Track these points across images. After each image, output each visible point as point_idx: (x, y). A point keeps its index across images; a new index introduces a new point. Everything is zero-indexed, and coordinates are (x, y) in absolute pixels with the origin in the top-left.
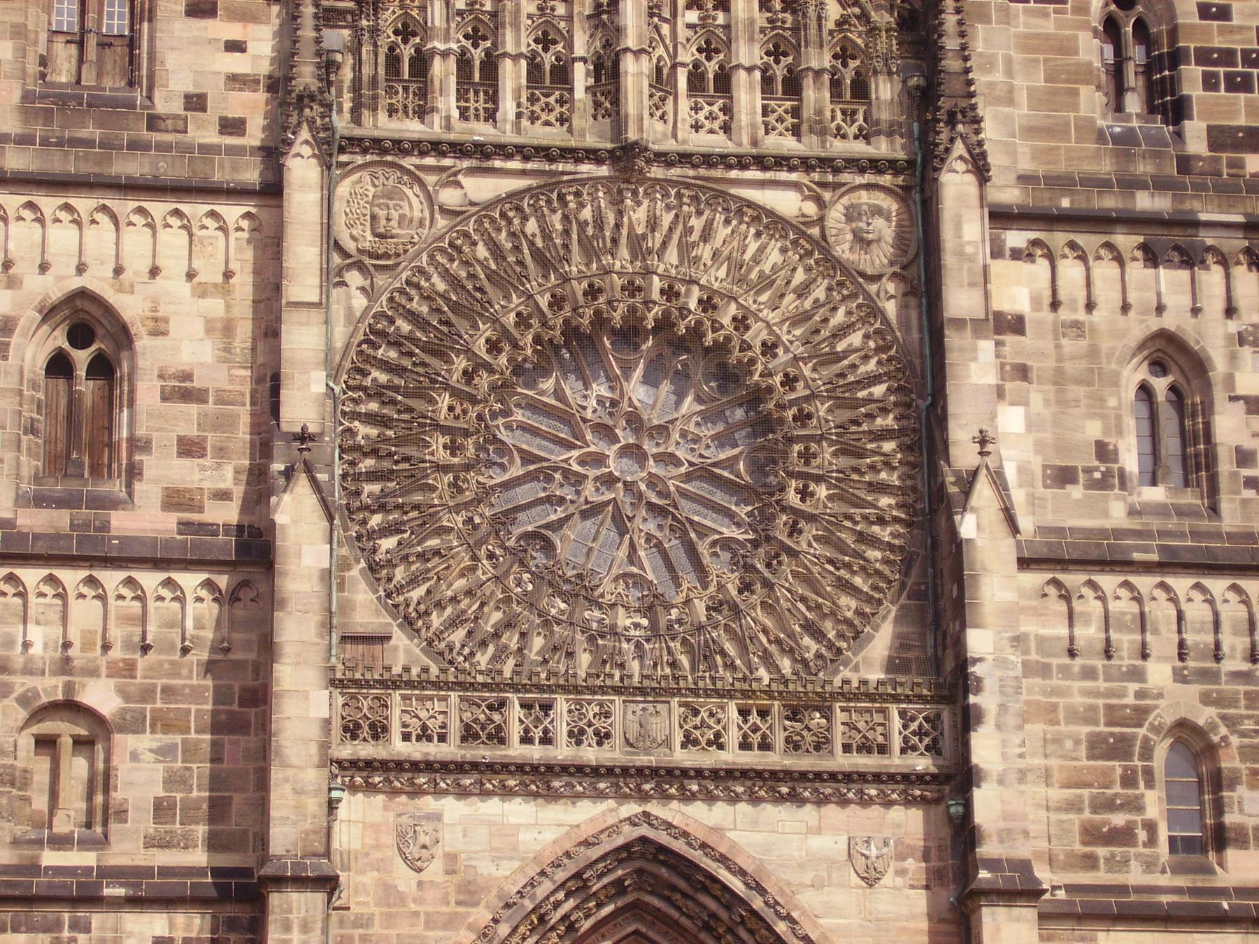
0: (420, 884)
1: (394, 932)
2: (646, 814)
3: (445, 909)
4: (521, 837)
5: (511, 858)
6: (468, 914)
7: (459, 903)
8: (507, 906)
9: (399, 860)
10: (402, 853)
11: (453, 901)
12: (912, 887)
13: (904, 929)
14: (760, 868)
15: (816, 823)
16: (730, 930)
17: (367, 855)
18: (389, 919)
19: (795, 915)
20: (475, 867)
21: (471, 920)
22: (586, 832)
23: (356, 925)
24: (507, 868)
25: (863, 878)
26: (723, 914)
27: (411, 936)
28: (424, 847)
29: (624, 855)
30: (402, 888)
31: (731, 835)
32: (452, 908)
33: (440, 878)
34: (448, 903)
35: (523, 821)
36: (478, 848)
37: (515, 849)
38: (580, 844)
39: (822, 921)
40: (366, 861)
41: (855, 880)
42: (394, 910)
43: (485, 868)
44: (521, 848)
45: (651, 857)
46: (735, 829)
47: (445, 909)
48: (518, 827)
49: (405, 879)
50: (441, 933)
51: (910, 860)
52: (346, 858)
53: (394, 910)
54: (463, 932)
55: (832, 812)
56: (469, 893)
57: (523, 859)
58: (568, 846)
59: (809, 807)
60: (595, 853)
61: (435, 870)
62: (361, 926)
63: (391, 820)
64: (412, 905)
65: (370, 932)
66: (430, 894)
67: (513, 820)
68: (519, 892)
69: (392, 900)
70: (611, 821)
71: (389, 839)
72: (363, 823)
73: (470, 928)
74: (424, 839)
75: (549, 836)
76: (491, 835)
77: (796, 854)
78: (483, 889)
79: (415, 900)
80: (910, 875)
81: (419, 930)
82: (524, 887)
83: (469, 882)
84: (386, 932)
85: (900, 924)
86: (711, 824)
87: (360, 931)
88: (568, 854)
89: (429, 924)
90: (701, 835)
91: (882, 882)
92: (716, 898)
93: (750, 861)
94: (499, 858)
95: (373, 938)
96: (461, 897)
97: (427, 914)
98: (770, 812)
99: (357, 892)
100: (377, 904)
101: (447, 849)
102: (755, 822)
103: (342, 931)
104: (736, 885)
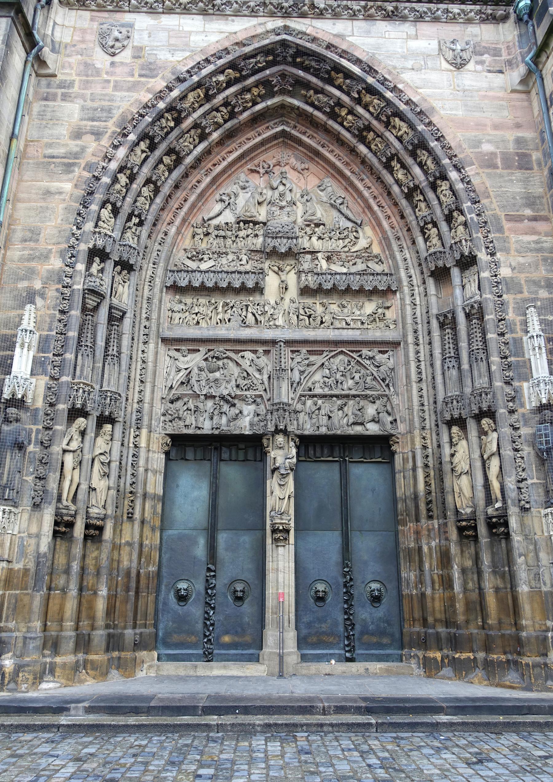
0: (113, 64)
1: (88, 92)
2: (286, 27)
3: (130, 79)
4: (192, 38)
5: (183, 50)
6: (148, 82)
7: (141, 76)
8: (180, 80)
9: (98, 49)
10: (103, 46)
11: (136, 75)
12: (489, 71)
13: (485, 96)
14: (373, 57)
15: (414, 33)
16: (351, 112)
17: (74, 46)
18: (86, 84)
19: (400, 86)
20: (156, 55)
21: (149, 86)
22: (240, 37)
23: (60, 86)
24: (179, 56)
25: (451, 64)
26: (345, 99)
27: (102, 95)
28: (117, 40)
29: (271, 58)
30: (98, 65)
31: (350, 39)
32: (136, 78)
33: (128, 60)
34: (133, 75)
35: (194, 29)
36: (159, 44)
37: (187, 45)
38: (237, 44)
39: (420, 91)
40: (73, 49)
41: (445, 65)
42: (90, 78)
43: (164, 56)
44: (192, 44)
45: (290, 59)
46: (353, 35)
47: (130, 79)
48: (190, 33)
49: (101, 59)
50: (126, 94)
51: (486, 56)
52: (57, 46)
53: (90, 78)
54: (142, 93)
55: (426, 28)
56: (150, 70)
57: (192, 51)
58: (227, 44)
59: (407, 25)
60: (247, 49)
61: (126, 56)
62: (64, 87)
63: (95, 27)
64: (105, 76)
65: (70, 91)
66: (118, 70)
67: (186, 29)
68: (188, 72)
69: (90, 72)
70: (260, 30)
71: (92, 37)
72: (75, 28)
73: (149, 91)
74: (116, 34)
75: (213, 38)
76: (169, 37)
77: (400, 50)
78: (160, 68)
79: (107, 73)
80: (487, 64)
81: (109, 90)
82: (192, 68)
83: (150, 63)
84: (83, 92)
85: (483, 93)
86: (334, 33)
87: (63, 90)
88: (227, 51)
89: (116, 87)
90: (328, 39)
91: (466, 67)
92: (339, 88)
93: (365, 54)
94: (174, 50)
95: (73, 95)
96: (143, 72)
97: (116, 81)
98: (382, 26)
99: (63, 67)
100: (78, 75)
101: (135, 44)
102: (369, 32)
103: (48, 90)
104: (356, 69)
